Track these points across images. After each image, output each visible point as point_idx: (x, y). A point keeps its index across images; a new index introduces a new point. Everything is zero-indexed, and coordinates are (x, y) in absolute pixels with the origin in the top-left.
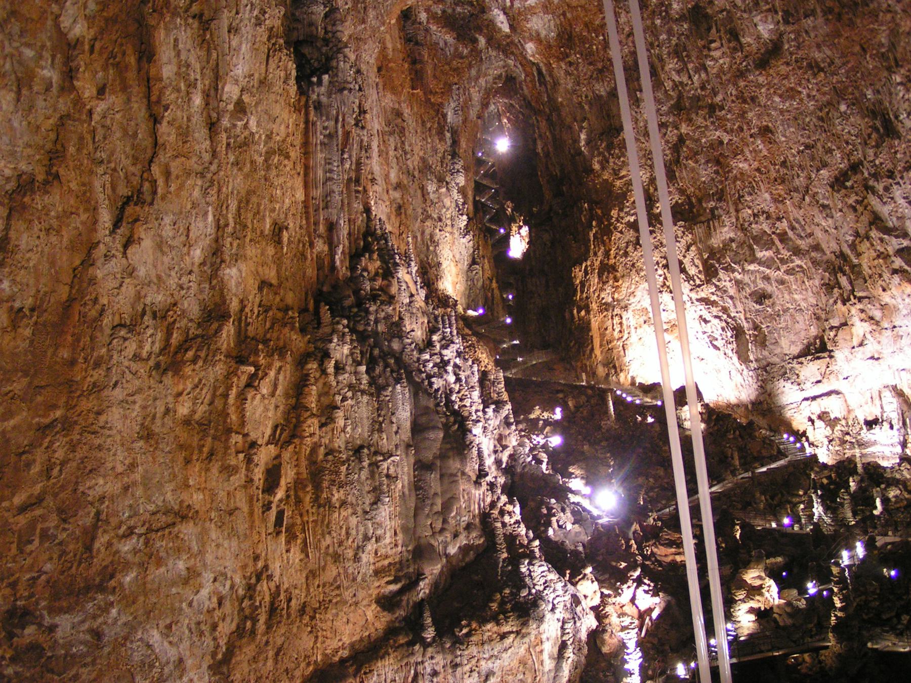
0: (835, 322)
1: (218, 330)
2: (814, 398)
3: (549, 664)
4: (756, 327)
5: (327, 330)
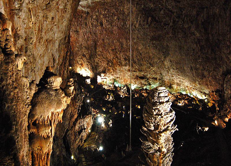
4: (96, 67)
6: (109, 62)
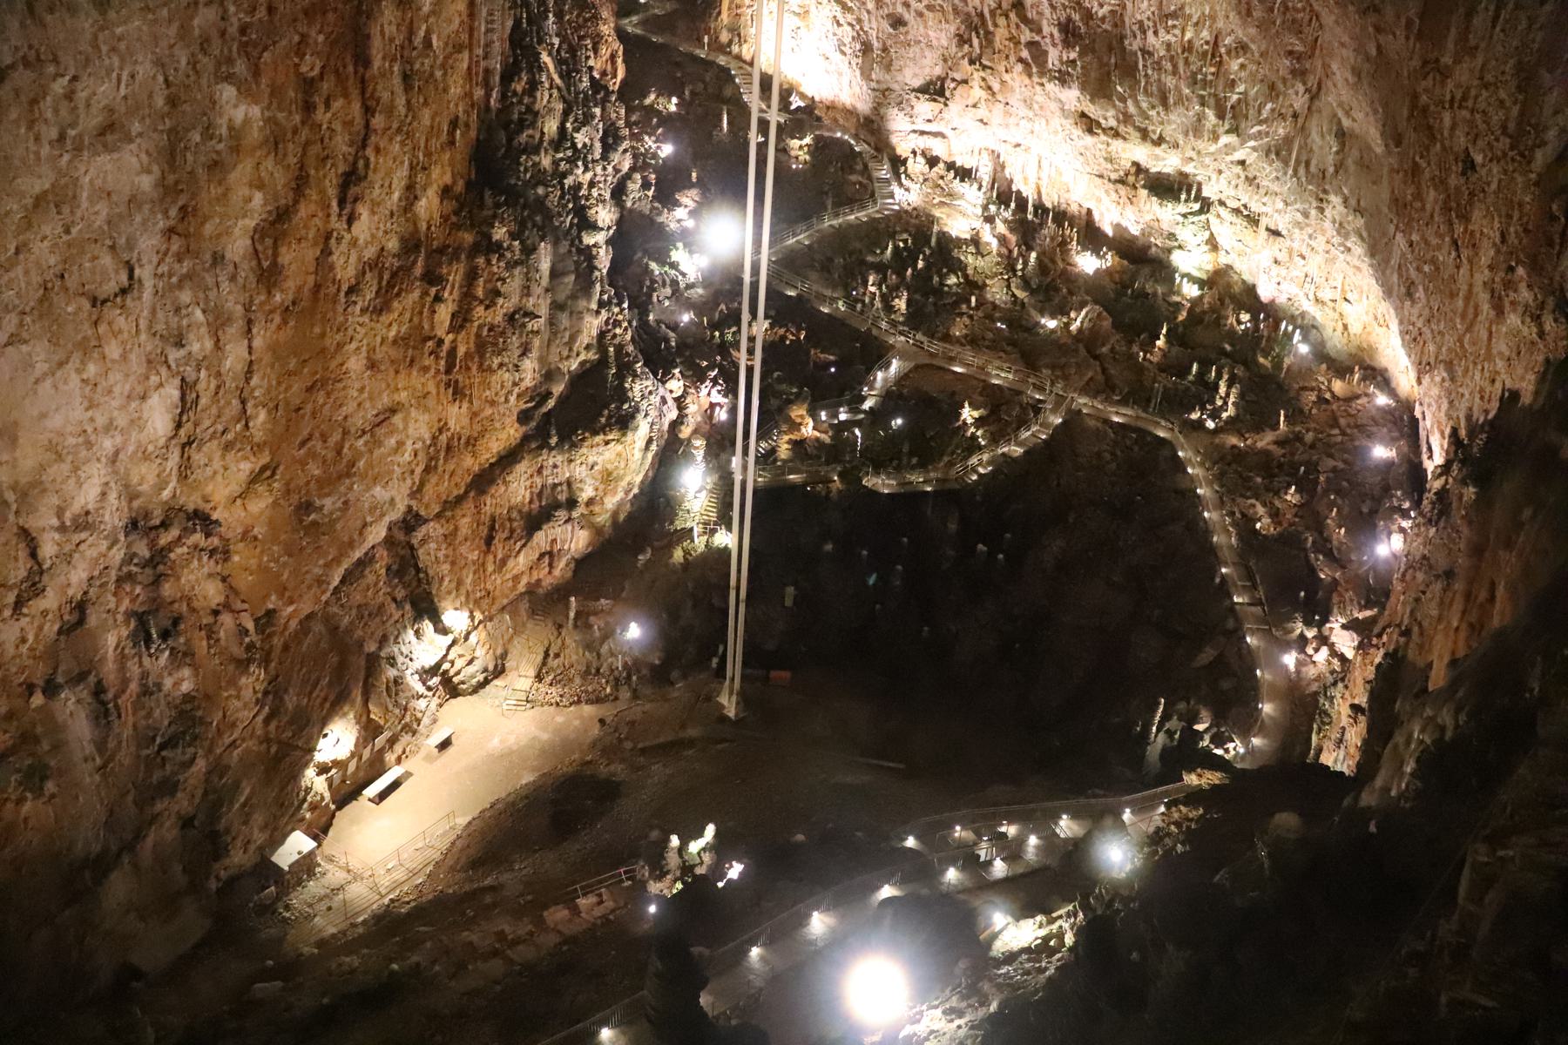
0: (958, 76)
1: (414, 262)
2: (923, 133)
3: (638, 455)
4: (885, 49)
5: (487, 213)
6: (972, 28)
